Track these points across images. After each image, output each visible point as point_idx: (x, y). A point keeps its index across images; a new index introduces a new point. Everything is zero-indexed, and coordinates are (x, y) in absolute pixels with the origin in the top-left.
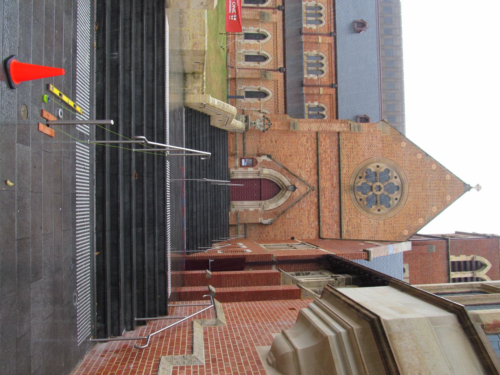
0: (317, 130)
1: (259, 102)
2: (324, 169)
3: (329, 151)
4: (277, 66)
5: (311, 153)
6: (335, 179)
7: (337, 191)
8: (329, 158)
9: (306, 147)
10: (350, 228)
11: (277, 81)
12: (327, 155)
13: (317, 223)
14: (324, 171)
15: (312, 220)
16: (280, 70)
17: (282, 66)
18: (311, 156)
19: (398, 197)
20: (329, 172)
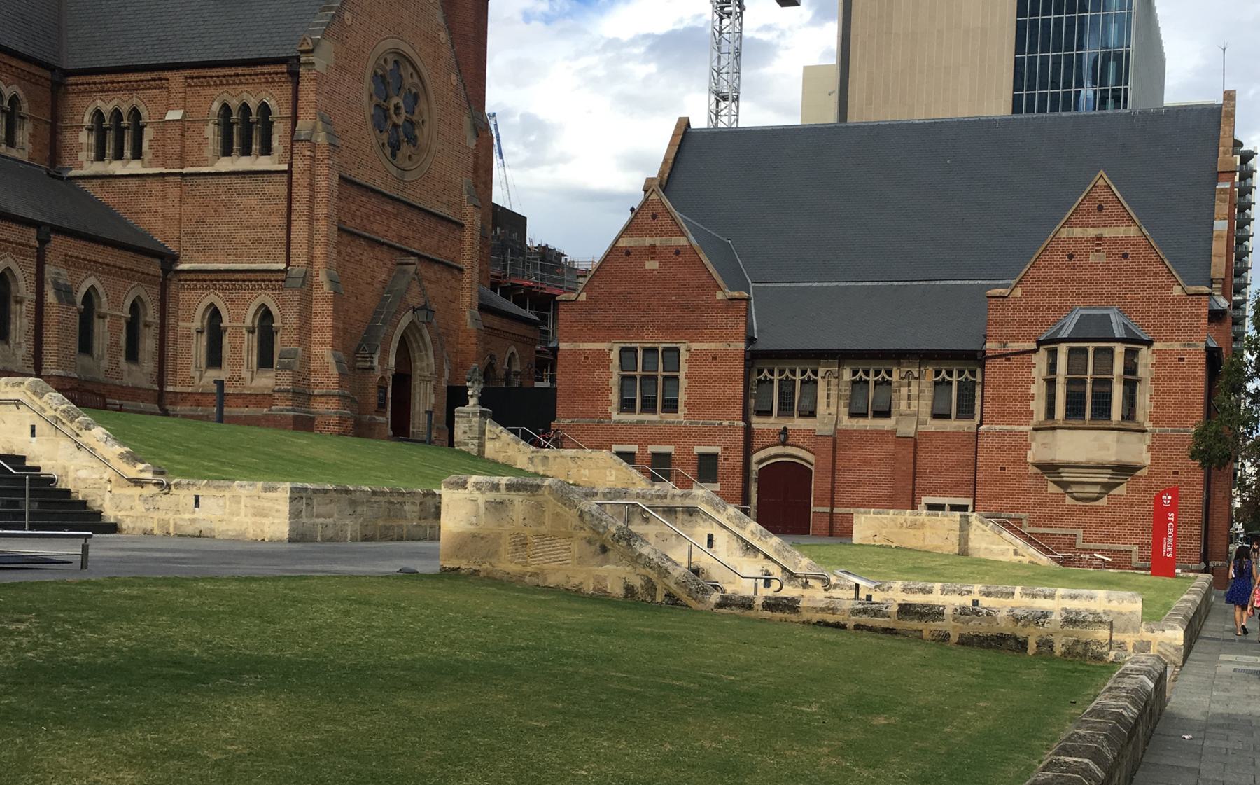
0: (336, 228)
1: (108, 319)
2: (375, 227)
3: (353, 207)
4: (31, 247)
5: (354, 249)
6: (388, 208)
7: (403, 209)
8: (362, 209)
9: (347, 258)
10: (445, 199)
11: (66, 255)
12: (358, 213)
13: (436, 267)
14: (378, 229)
15: (433, 274)
16: (43, 241)
17: (33, 233)
18: (359, 251)
19: (411, 70)
20: (378, 218)
